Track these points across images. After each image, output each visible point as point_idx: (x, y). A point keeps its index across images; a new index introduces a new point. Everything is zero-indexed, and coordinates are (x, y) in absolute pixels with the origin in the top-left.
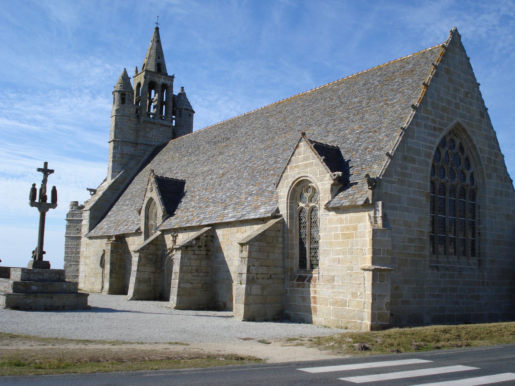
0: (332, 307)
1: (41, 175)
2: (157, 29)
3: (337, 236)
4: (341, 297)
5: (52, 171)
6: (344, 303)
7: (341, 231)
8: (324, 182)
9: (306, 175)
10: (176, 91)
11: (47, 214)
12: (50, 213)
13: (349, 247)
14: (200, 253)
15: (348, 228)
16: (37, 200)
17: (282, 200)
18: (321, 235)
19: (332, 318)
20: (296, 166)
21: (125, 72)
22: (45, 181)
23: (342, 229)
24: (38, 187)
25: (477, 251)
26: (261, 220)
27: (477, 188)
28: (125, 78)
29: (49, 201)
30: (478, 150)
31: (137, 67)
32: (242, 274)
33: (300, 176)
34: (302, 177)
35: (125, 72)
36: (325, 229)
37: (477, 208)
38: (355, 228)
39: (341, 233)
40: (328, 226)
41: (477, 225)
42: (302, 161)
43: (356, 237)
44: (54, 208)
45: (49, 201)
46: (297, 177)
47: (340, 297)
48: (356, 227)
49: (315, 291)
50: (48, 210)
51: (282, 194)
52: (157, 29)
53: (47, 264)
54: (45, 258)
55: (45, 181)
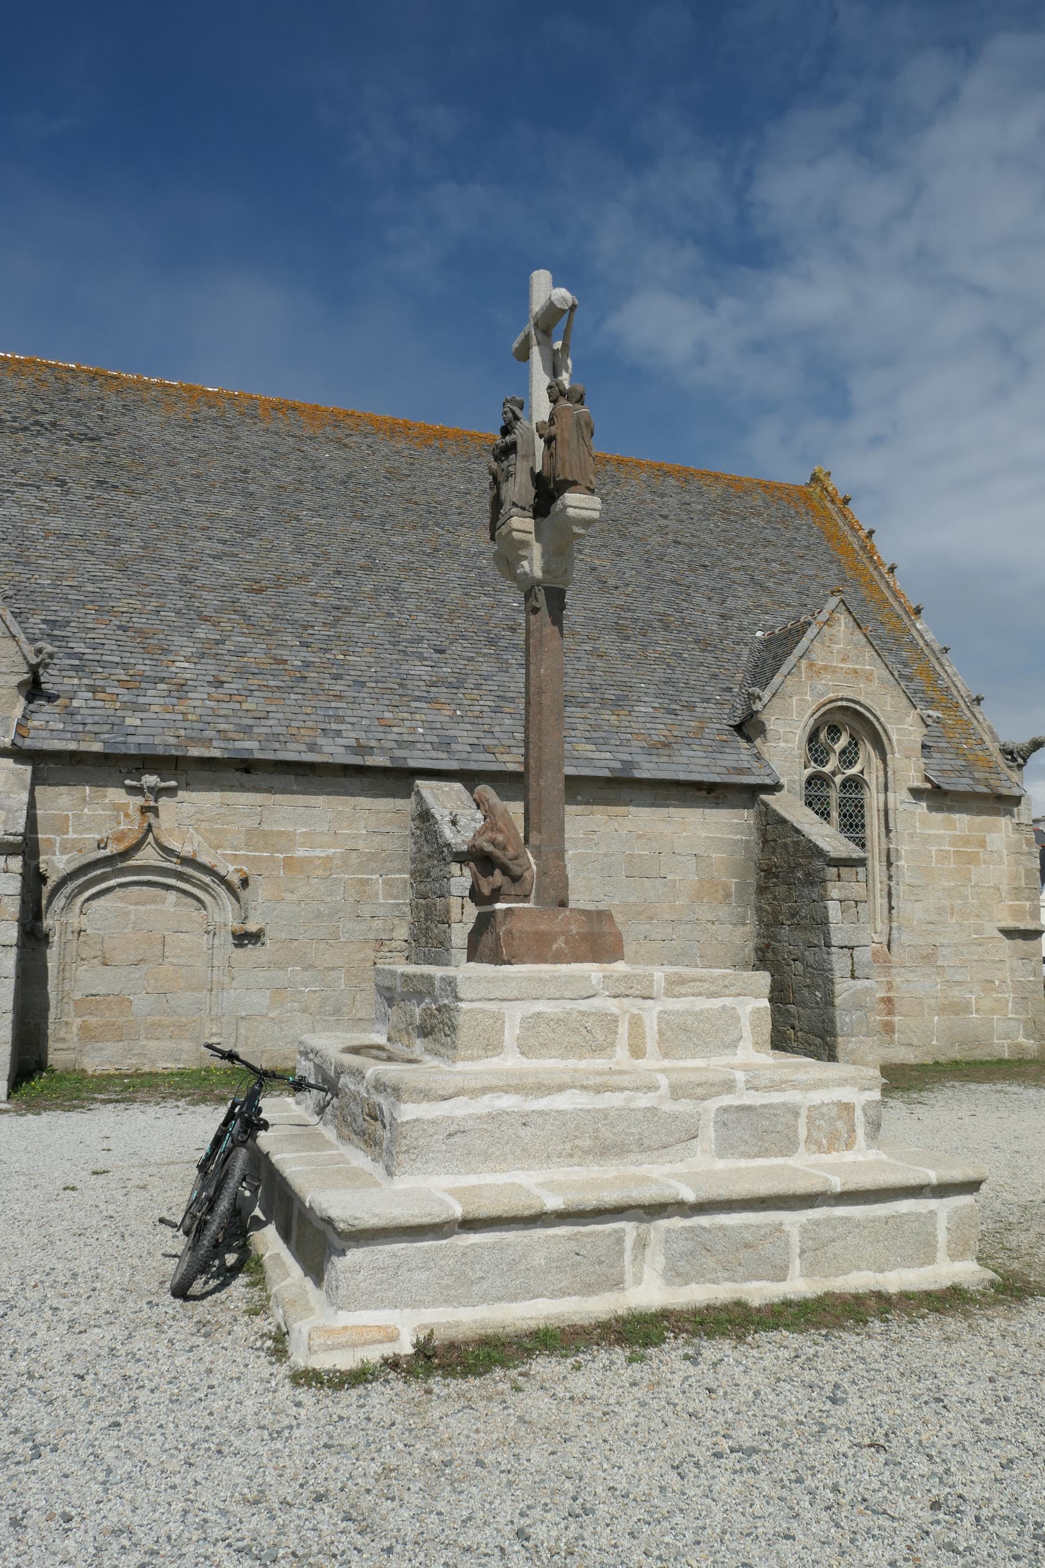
0: (936, 1018)
3: (944, 856)
4: (955, 993)
6: (959, 1008)
7: (953, 845)
8: (906, 726)
9: (856, 698)
13: (970, 880)
15: (966, 841)
17: (782, 744)
18: (903, 853)
19: (934, 1042)
20: (825, 668)
23: (955, 840)
26: (699, 789)
32: (852, 948)
33: (840, 695)
34: (841, 699)
36: (911, 836)
38: (983, 844)
39: (952, 849)
40: (918, 831)
42: (843, 660)
43: (985, 862)
46: (832, 695)
47: (957, 993)
48: (985, 842)
49: (888, 982)
51: (781, 731)
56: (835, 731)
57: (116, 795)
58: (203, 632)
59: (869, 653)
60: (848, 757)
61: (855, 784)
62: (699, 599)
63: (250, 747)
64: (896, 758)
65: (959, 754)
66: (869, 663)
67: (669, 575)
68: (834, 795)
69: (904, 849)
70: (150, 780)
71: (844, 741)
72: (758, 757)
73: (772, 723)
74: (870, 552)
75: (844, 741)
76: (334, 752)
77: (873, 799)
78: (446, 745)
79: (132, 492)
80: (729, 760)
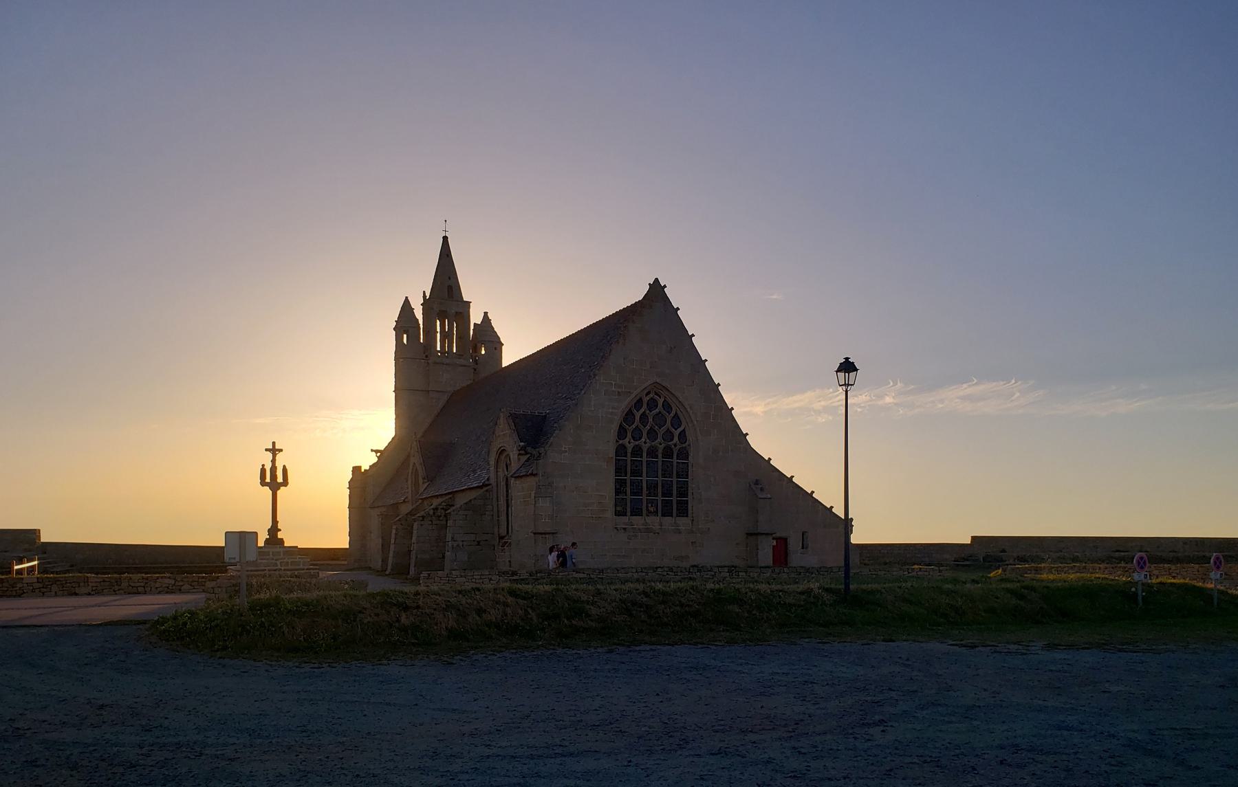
1: (270, 455)
2: (445, 239)
5: (281, 450)
10: (476, 318)
11: (278, 492)
12: (282, 492)
14: (438, 522)
16: (268, 480)
21: (407, 301)
22: (273, 461)
24: (268, 467)
25: (690, 512)
27: (689, 445)
28: (407, 307)
29: (280, 479)
30: (687, 407)
31: (424, 292)
35: (407, 301)
37: (690, 467)
41: (689, 484)
44: (286, 486)
45: (280, 479)
46: (499, 447)
50: (279, 489)
52: (445, 239)
53: (282, 541)
54: (280, 535)
55: (273, 461)
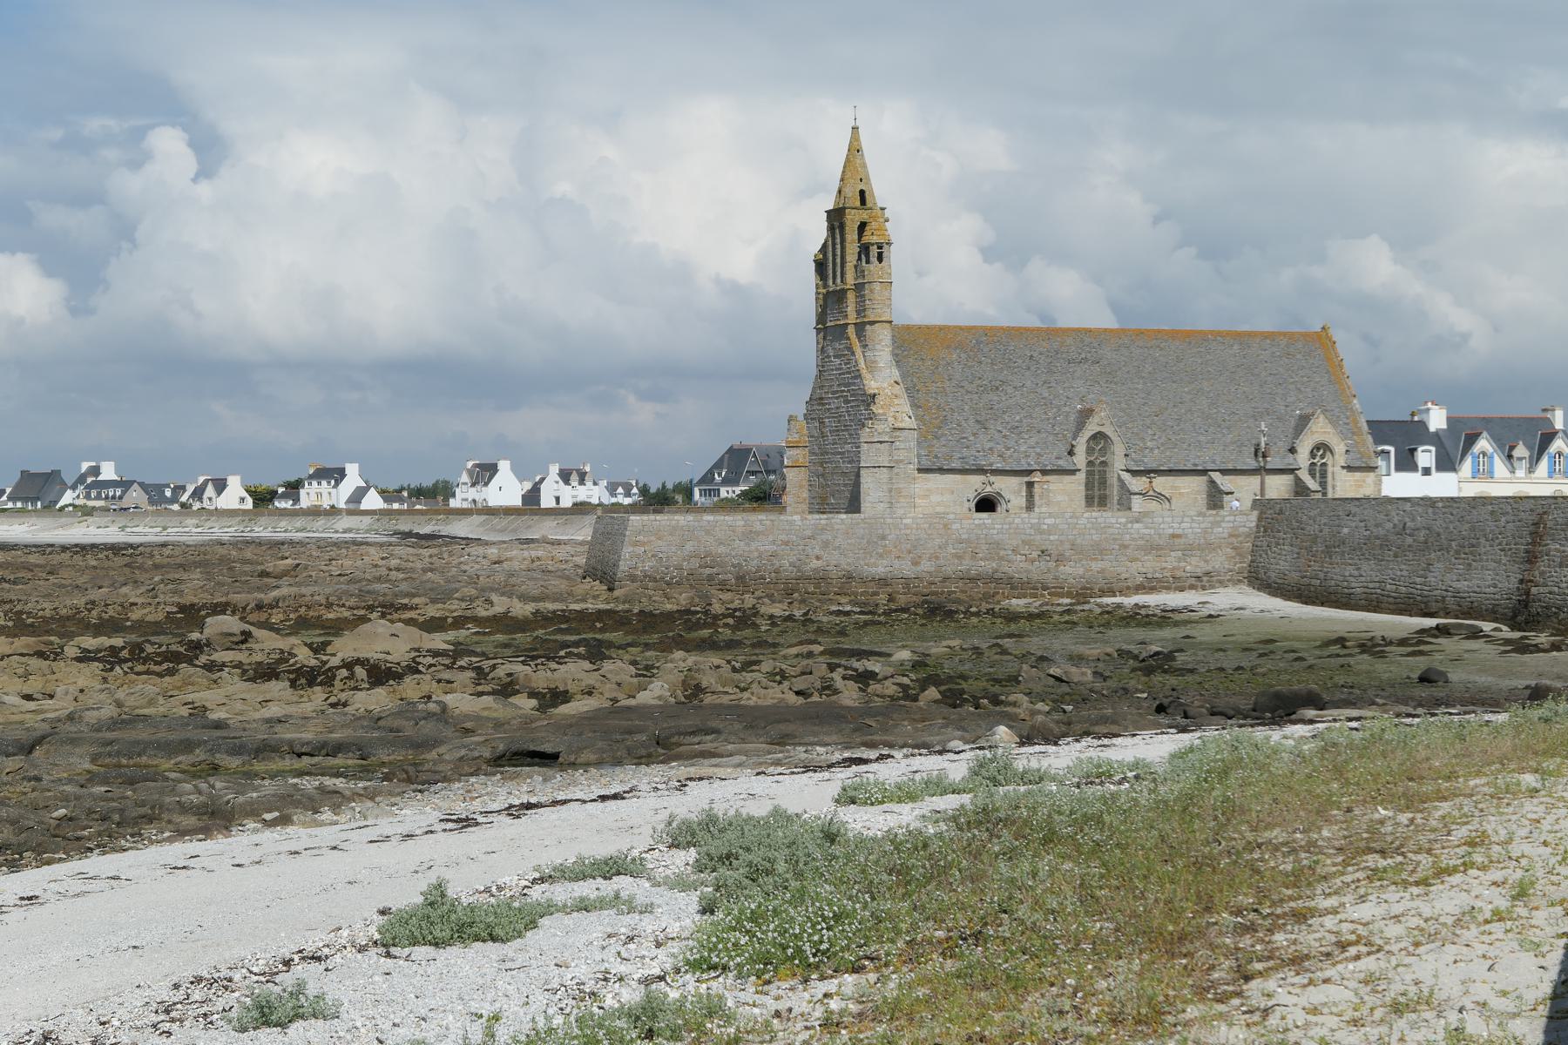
15: (1357, 481)
38: (1364, 481)
56: (1318, 449)
57: (1144, 479)
58: (1150, 432)
59: (1329, 426)
60: (1322, 457)
61: (1324, 464)
62: (1278, 399)
63: (1172, 466)
64: (1336, 457)
65: (1360, 453)
66: (1329, 429)
67: (1269, 391)
68: (1318, 468)
69: (1338, 484)
70: (1152, 475)
71: (1321, 452)
72: (1295, 459)
73: (1299, 450)
74: (1341, 367)
75: (1321, 452)
76: (1189, 467)
77: (1330, 469)
78: (1214, 462)
79: (1116, 384)
80: (1286, 461)
